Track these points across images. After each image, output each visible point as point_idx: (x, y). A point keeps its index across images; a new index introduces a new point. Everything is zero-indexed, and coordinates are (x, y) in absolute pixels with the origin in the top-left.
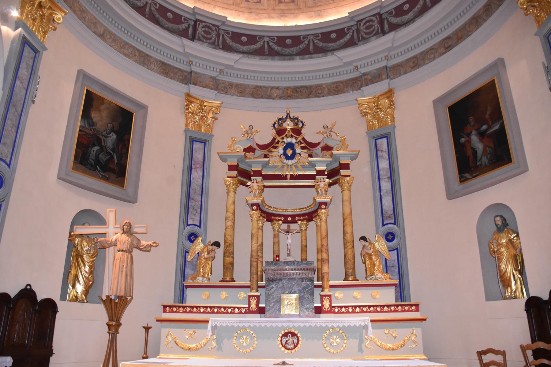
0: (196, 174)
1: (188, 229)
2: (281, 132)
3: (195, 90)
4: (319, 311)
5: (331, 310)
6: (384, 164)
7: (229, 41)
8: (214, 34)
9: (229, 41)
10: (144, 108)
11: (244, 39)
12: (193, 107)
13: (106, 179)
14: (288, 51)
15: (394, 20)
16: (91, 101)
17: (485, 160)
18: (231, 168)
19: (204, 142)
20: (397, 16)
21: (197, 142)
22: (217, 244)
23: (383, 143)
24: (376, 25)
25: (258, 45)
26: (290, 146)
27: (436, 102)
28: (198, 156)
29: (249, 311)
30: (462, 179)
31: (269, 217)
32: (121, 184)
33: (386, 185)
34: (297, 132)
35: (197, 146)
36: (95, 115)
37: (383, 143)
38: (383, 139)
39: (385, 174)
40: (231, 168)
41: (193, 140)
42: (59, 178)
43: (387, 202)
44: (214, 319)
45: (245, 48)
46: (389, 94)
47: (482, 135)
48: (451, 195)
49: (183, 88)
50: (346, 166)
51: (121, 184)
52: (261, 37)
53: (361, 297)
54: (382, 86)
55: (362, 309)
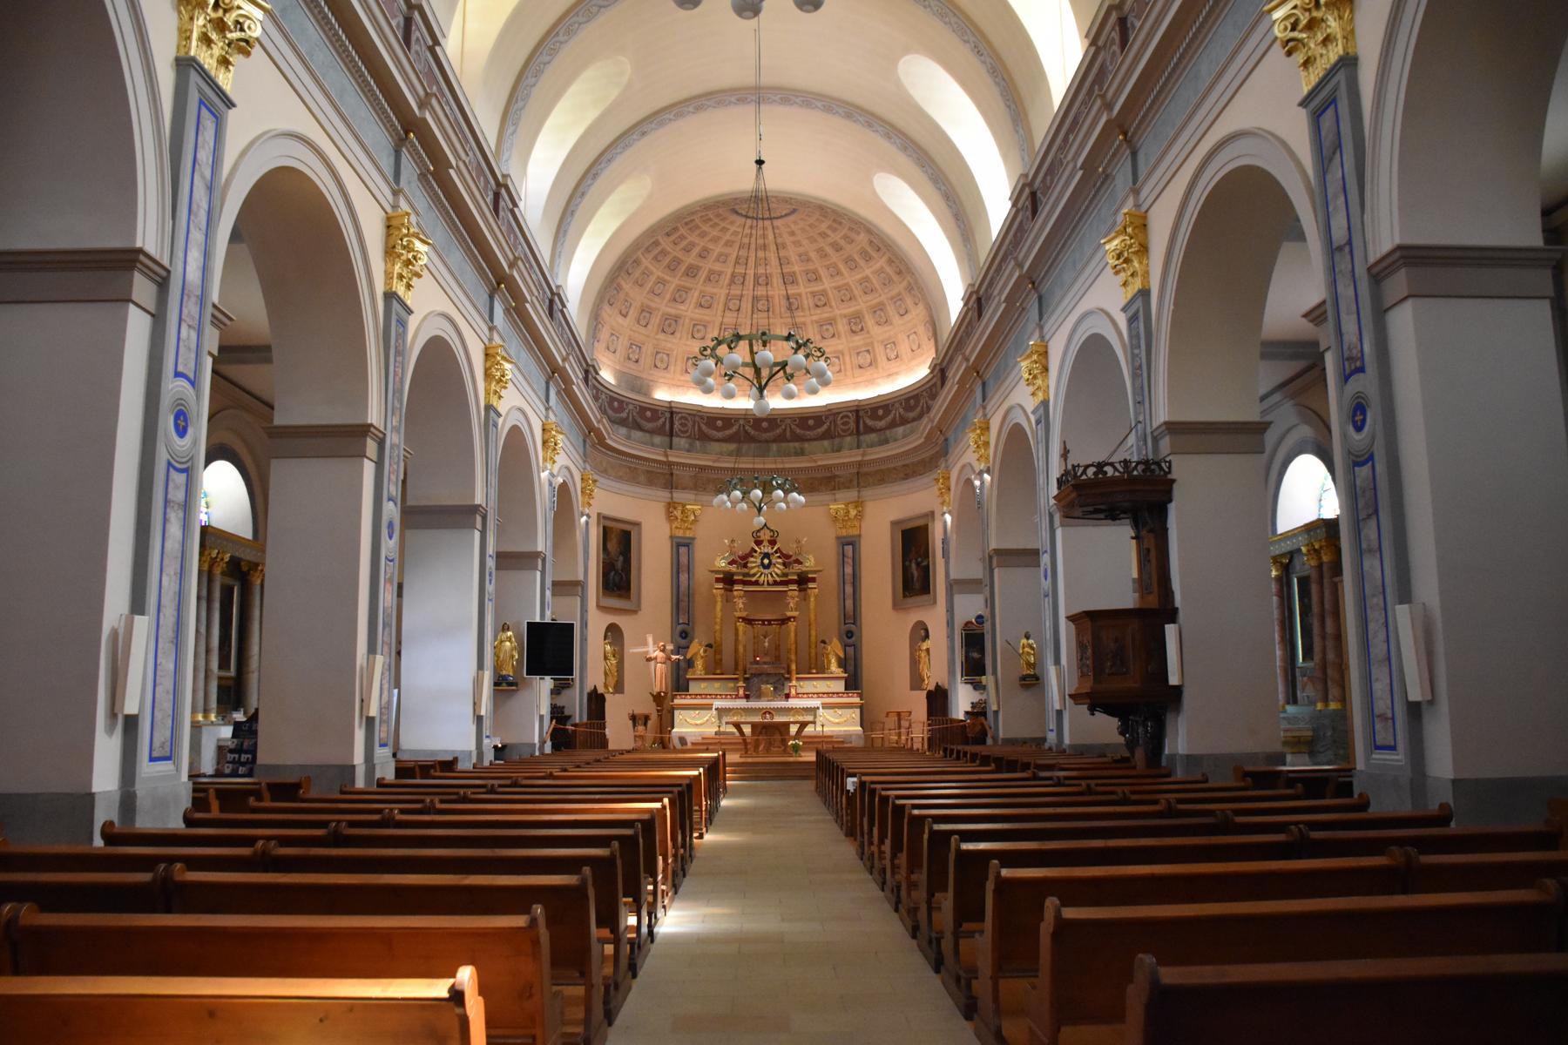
0: (684, 577)
1: (680, 628)
2: (759, 543)
3: (679, 496)
4: (788, 696)
5: (798, 695)
6: (849, 570)
7: (704, 427)
8: (690, 424)
9: (704, 427)
10: (637, 524)
11: (719, 423)
12: (678, 513)
13: (620, 596)
14: (766, 436)
15: (870, 422)
16: (606, 533)
17: (917, 586)
18: (718, 580)
19: (687, 545)
20: (871, 417)
21: (682, 545)
22: (710, 646)
23: (849, 549)
24: (852, 425)
25: (734, 429)
26: (767, 555)
27: (894, 524)
28: (684, 560)
29: (737, 697)
30: (905, 596)
31: (748, 621)
32: (628, 597)
33: (849, 589)
34: (773, 543)
35: (683, 550)
36: (609, 546)
37: (849, 549)
38: (849, 546)
39: (849, 578)
40: (718, 580)
41: (679, 545)
42: (599, 607)
43: (849, 603)
44: (718, 703)
45: (720, 435)
46: (859, 504)
47: (918, 564)
48: (896, 606)
49: (664, 495)
50: (813, 580)
51: (628, 597)
52: (737, 420)
53: (821, 686)
54: (852, 494)
55: (819, 695)
